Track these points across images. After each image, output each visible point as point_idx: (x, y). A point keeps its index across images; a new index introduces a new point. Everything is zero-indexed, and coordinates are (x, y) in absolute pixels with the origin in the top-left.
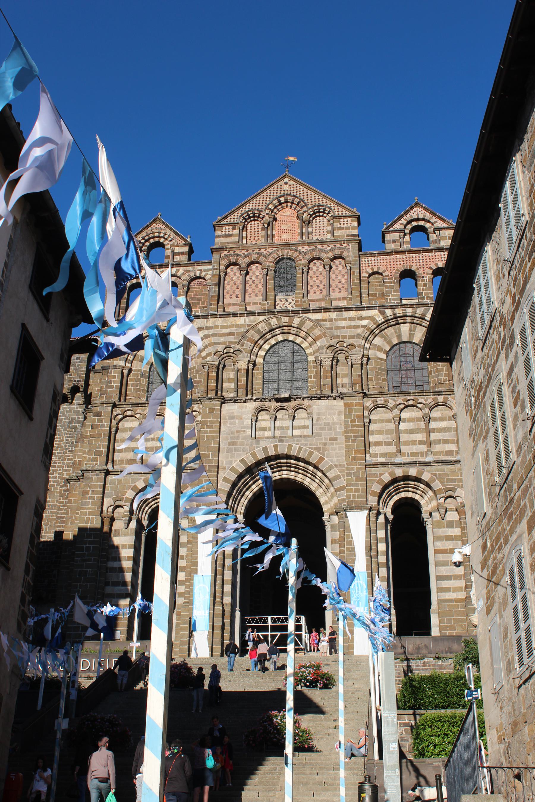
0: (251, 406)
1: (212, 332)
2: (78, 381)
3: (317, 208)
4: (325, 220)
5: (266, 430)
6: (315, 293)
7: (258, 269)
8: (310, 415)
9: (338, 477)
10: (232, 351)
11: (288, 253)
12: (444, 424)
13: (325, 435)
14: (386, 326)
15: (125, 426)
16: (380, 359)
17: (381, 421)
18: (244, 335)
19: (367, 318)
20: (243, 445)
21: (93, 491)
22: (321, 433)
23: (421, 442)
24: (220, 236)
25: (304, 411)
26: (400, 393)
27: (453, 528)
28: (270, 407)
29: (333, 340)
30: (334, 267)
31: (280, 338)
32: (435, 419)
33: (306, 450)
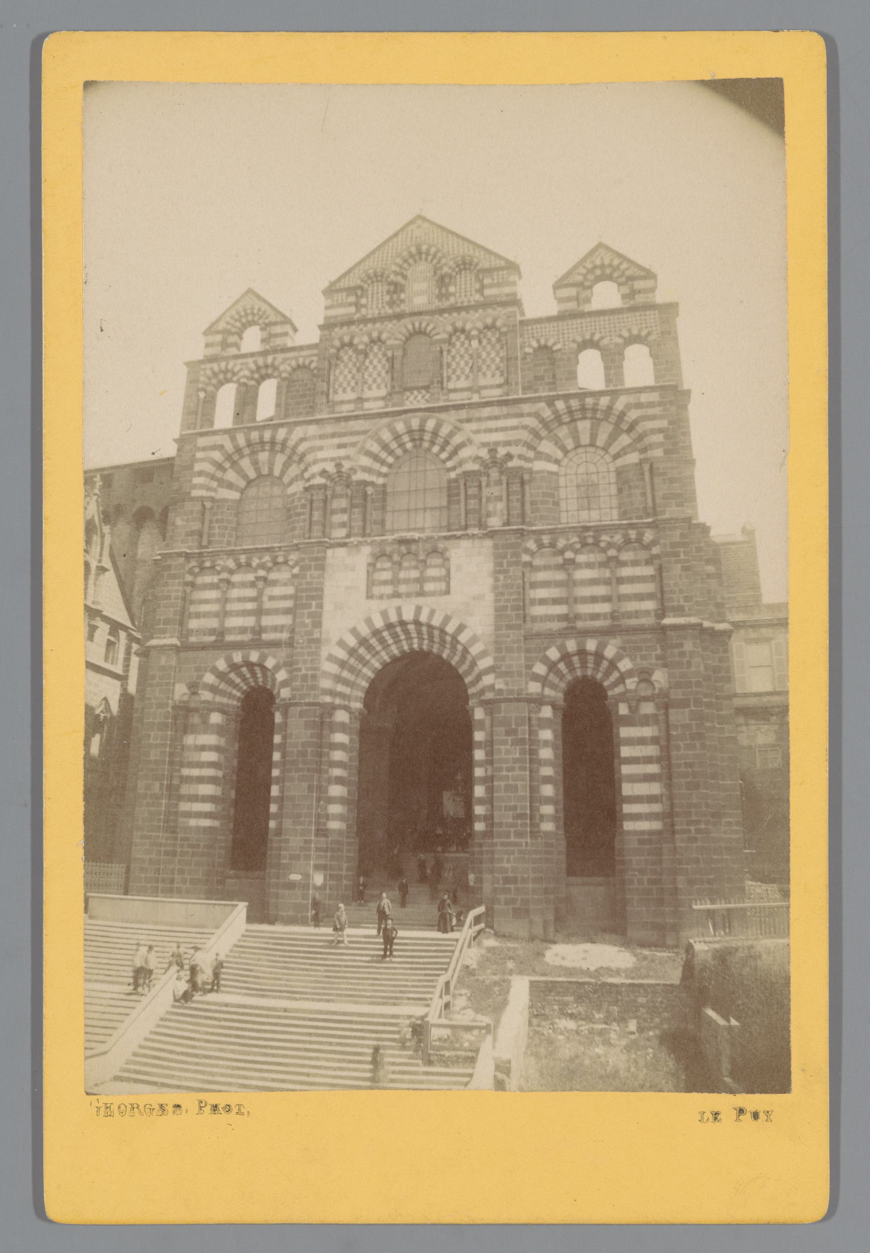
12: (639, 571)
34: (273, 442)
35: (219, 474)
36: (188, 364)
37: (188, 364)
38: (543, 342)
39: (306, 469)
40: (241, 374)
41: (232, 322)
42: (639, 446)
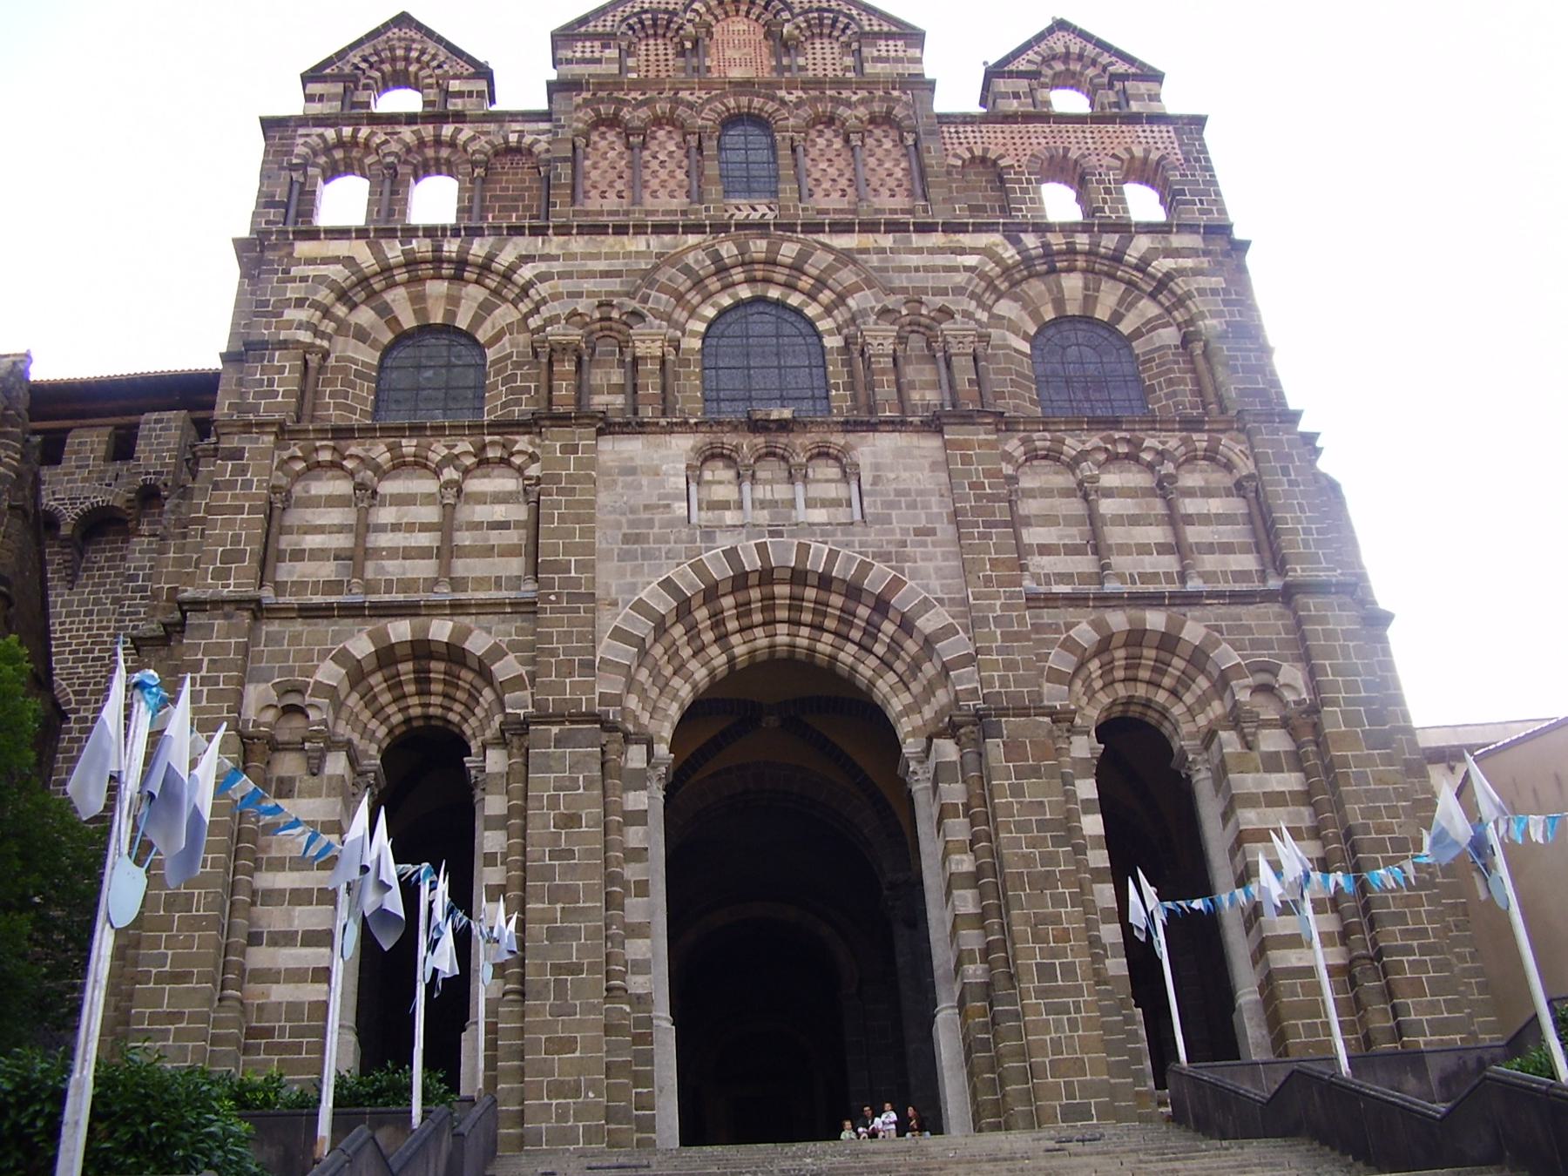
0: (683, 444)
1: (557, 267)
2: (154, 473)
3: (816, 15)
4: (836, 45)
5: (729, 508)
6: (828, 195)
7: (672, 138)
8: (849, 473)
9: (948, 631)
10: (615, 314)
11: (750, 102)
12: (1215, 505)
13: (901, 522)
14: (1025, 273)
15: (313, 492)
16: (1016, 350)
17: (1046, 493)
18: (648, 277)
19: (974, 251)
20: (668, 542)
21: (211, 661)
22: (890, 515)
23: (1163, 549)
24: (569, 61)
25: (831, 462)
26: (1096, 423)
27: (1282, 771)
28: (737, 449)
29: (893, 298)
30: (870, 141)
31: (745, 293)
32: (1190, 493)
33: (850, 559)
34: (461, 263)
35: (341, 310)
36: (270, 125)
37: (270, 125)
38: (978, 152)
39: (536, 310)
40: (385, 149)
41: (364, 65)
42: (1179, 315)
